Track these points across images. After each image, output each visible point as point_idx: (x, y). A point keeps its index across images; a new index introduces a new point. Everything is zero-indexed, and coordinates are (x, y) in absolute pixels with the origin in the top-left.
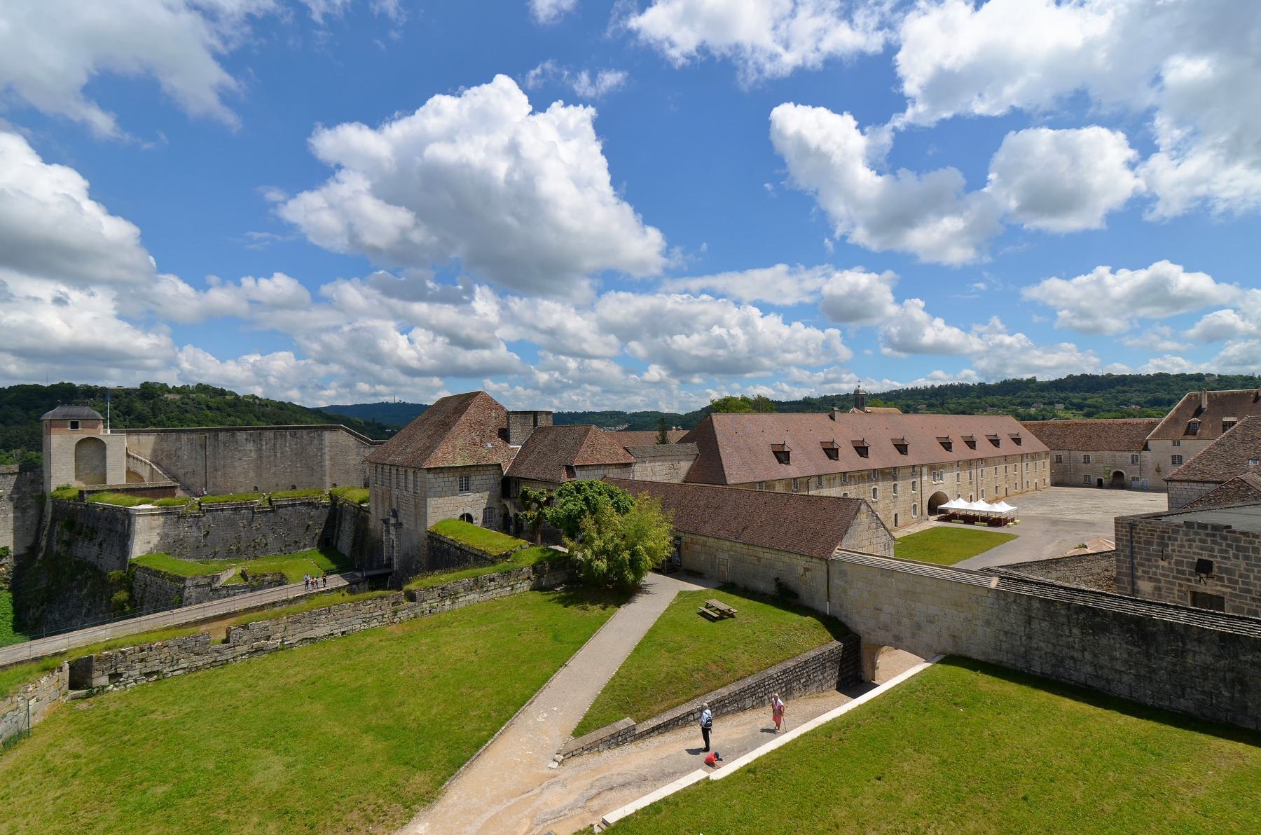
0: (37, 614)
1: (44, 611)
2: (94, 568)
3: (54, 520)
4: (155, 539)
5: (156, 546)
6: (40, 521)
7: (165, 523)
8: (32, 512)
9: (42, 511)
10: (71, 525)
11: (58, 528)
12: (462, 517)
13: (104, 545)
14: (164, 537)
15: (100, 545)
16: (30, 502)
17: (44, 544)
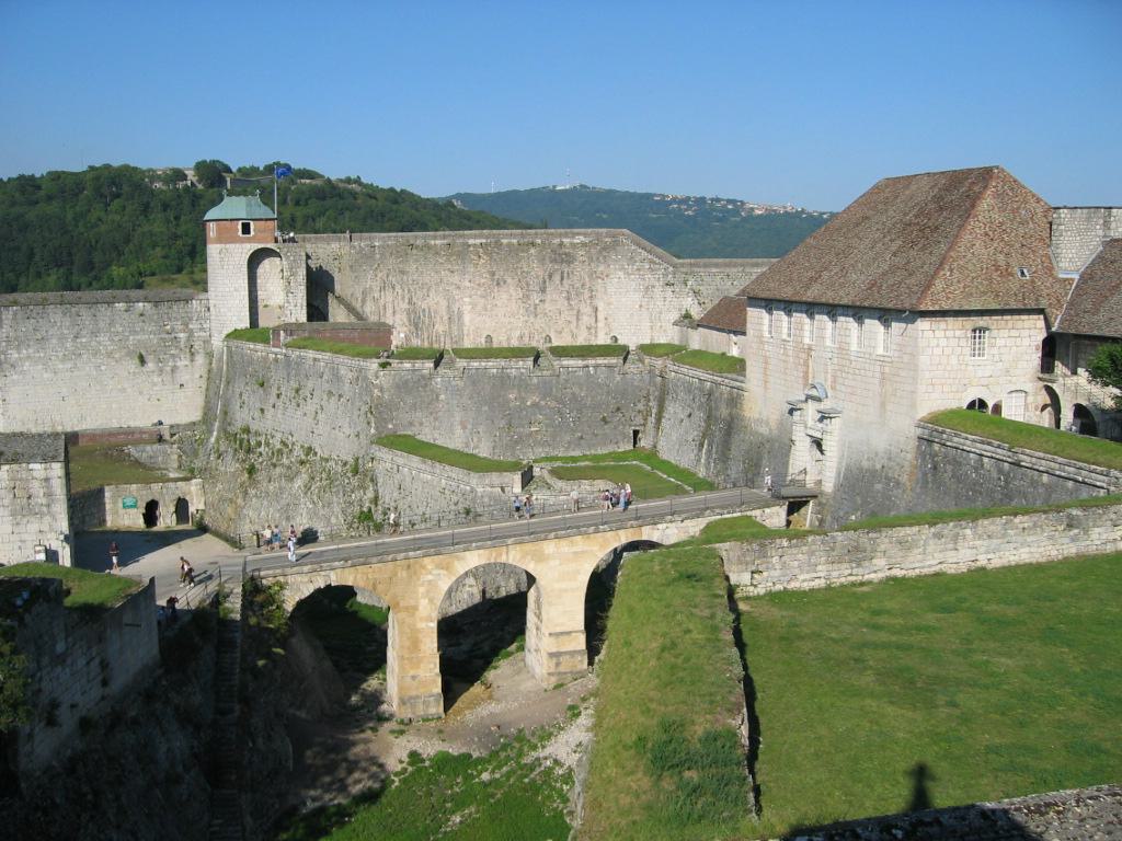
8: (200, 359)
12: (971, 405)
13: (321, 416)
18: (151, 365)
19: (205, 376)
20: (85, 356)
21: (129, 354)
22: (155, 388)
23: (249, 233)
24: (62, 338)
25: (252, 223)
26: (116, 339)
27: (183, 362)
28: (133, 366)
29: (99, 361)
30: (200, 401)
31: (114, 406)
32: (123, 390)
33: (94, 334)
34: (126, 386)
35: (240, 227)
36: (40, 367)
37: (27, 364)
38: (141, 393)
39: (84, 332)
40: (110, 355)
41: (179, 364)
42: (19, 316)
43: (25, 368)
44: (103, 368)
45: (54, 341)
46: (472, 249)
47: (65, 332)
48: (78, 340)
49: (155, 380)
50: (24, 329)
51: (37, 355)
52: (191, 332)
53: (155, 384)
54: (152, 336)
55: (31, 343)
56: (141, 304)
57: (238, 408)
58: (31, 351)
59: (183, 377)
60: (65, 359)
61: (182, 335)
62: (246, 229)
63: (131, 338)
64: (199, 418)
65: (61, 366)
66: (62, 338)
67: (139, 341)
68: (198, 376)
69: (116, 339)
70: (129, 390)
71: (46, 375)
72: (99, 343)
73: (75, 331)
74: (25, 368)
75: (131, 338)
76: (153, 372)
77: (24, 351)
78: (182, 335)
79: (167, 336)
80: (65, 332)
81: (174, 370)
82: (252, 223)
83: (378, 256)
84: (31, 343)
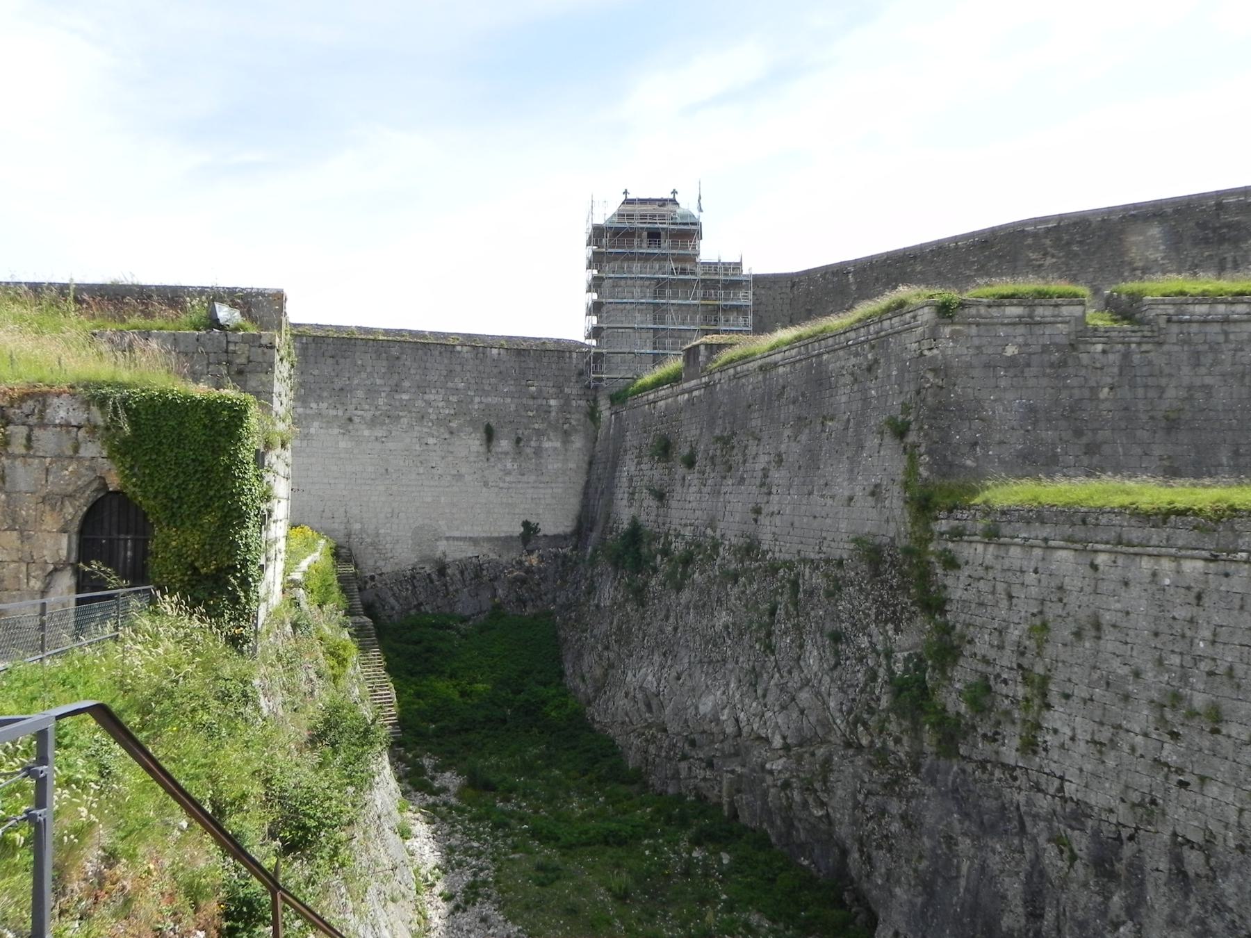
8: (578, 442)
18: (504, 444)
19: (585, 466)
20: (404, 421)
21: (472, 422)
22: (508, 479)
24: (372, 392)
26: (454, 399)
27: (552, 444)
28: (478, 442)
29: (426, 430)
30: (573, 504)
31: (443, 499)
32: (459, 477)
33: (422, 388)
34: (463, 471)
36: (336, 431)
37: (316, 424)
38: (486, 484)
39: (406, 384)
40: (442, 422)
41: (546, 444)
42: (310, 352)
43: (312, 431)
44: (431, 441)
45: (360, 394)
46: (1030, 241)
47: (378, 381)
48: (397, 397)
49: (509, 466)
50: (316, 372)
51: (332, 412)
52: (567, 399)
53: (509, 473)
54: (509, 400)
55: (325, 394)
57: (625, 502)
58: (324, 405)
59: (553, 465)
60: (373, 423)
61: (553, 402)
63: (477, 399)
64: (569, 530)
65: (366, 433)
66: (372, 392)
67: (487, 405)
68: (572, 465)
69: (454, 399)
70: (468, 478)
71: (342, 445)
72: (429, 403)
73: (393, 382)
74: (312, 431)
75: (477, 399)
76: (507, 453)
77: (314, 405)
78: (553, 402)
79: (531, 402)
80: (378, 381)
81: (538, 452)
83: (854, 287)
84: (325, 394)
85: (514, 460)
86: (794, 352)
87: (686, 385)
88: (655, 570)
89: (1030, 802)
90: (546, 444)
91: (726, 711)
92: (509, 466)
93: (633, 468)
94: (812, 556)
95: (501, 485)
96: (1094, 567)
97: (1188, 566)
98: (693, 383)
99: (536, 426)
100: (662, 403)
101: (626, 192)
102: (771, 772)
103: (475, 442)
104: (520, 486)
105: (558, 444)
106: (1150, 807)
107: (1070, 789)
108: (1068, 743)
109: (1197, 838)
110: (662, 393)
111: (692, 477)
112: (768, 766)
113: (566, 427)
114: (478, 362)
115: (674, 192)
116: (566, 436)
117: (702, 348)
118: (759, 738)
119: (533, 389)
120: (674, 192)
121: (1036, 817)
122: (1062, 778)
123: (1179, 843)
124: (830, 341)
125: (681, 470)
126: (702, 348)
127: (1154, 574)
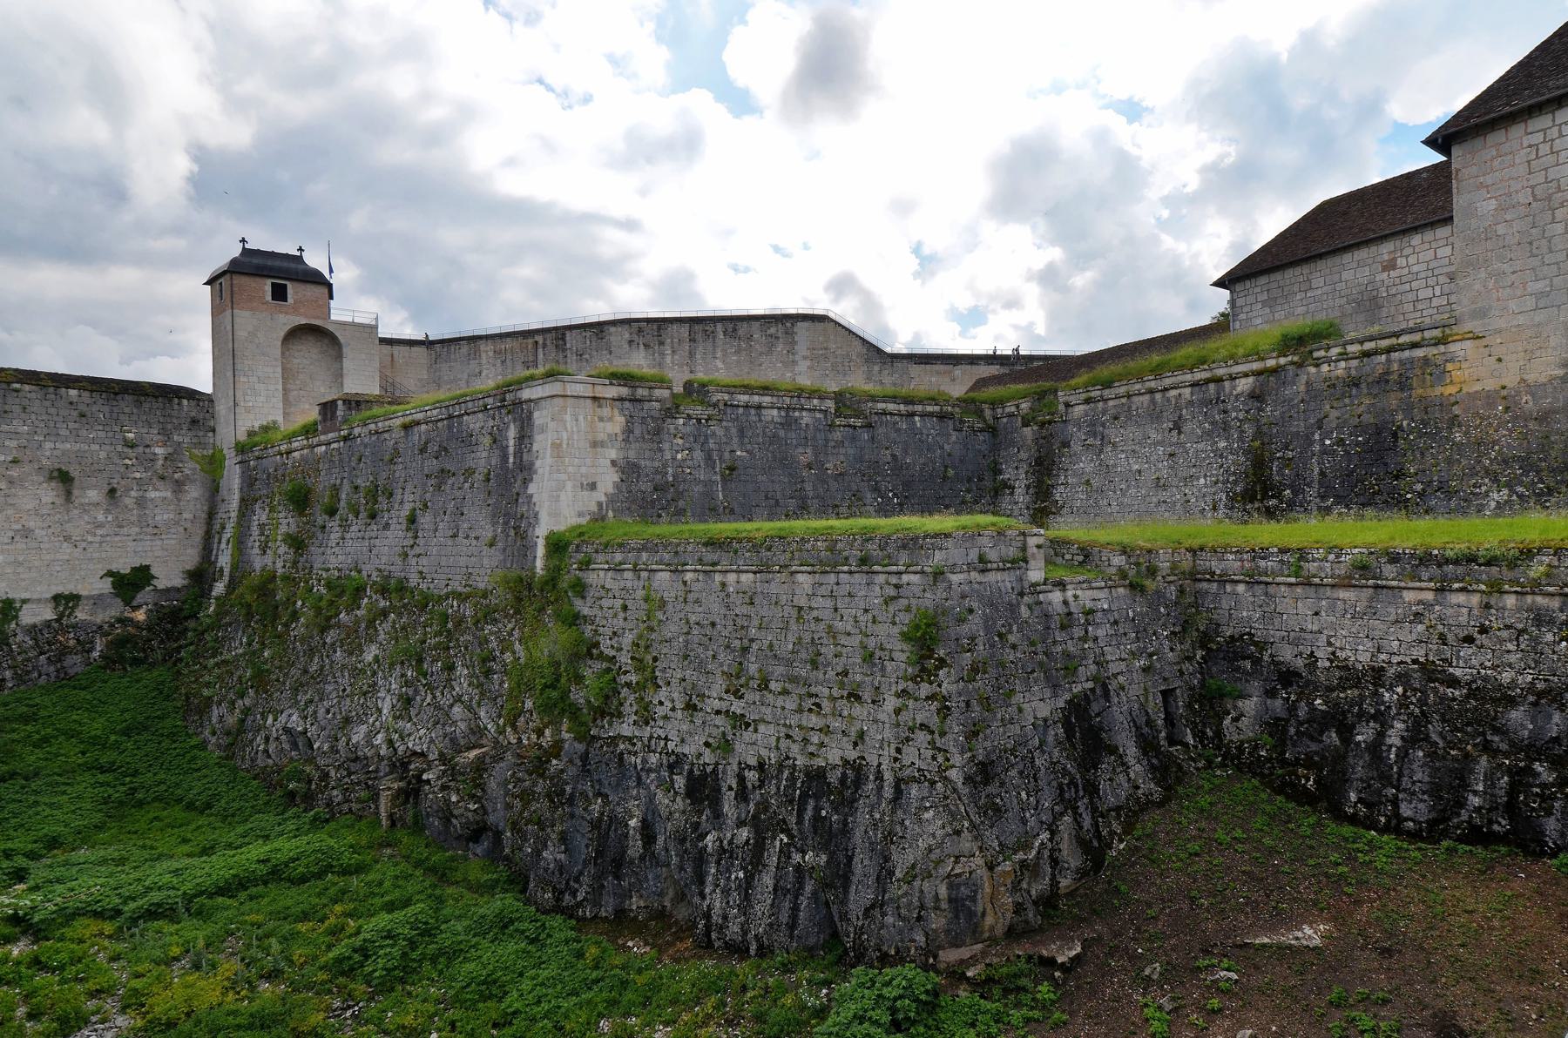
0: (231, 720)
1: (247, 711)
2: (392, 588)
3: (246, 504)
4: (608, 480)
5: (612, 499)
6: (211, 515)
7: (628, 431)
8: (194, 492)
9: (214, 492)
10: (300, 500)
11: (260, 515)
13: (425, 520)
14: (629, 470)
15: (412, 520)
16: (189, 467)
17: (224, 560)
22: (99, 532)
23: (285, 300)
25: (289, 285)
34: (31, 524)
35: (268, 288)
38: (67, 538)
53: (101, 526)
56: (73, 393)
57: (256, 551)
61: (159, 451)
62: (279, 293)
75: (48, 445)
78: (159, 451)
81: (141, 503)
82: (289, 285)
85: (107, 511)
86: (435, 412)
87: (323, 438)
88: (295, 616)
89: (645, 761)
90: (152, 494)
91: (379, 736)
92: (101, 518)
93: (264, 517)
94: (460, 589)
95: (90, 539)
96: (685, 583)
97: (744, 577)
98: (331, 435)
99: (138, 475)
100: (296, 454)
101: (243, 241)
102: (428, 781)
103: (49, 494)
104: (117, 539)
105: (168, 494)
106: (726, 746)
107: (671, 746)
108: (670, 714)
109: (753, 762)
110: (295, 445)
111: (334, 524)
112: (425, 777)
113: (176, 476)
114: (48, 403)
115: (301, 249)
116: (178, 486)
117: (340, 403)
118: (415, 753)
119: (131, 435)
120: (301, 249)
121: (650, 770)
122: (666, 739)
123: (743, 767)
124: (470, 405)
125: (321, 519)
126: (340, 403)
127: (723, 585)
